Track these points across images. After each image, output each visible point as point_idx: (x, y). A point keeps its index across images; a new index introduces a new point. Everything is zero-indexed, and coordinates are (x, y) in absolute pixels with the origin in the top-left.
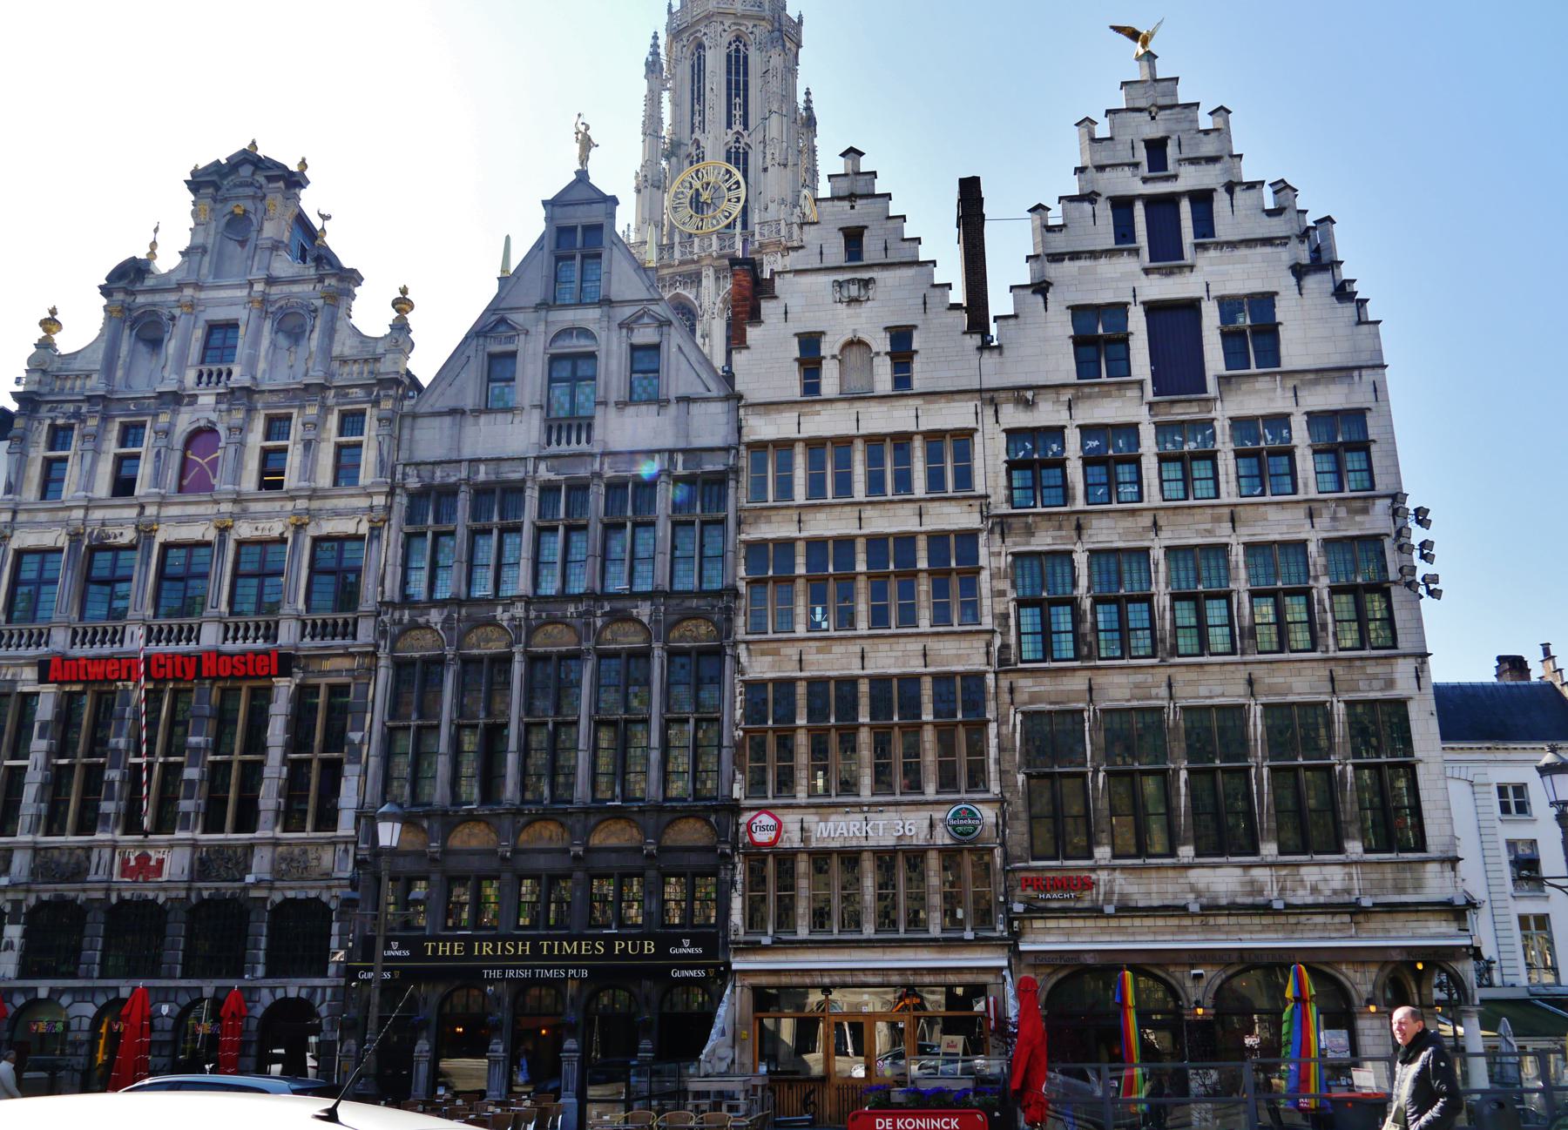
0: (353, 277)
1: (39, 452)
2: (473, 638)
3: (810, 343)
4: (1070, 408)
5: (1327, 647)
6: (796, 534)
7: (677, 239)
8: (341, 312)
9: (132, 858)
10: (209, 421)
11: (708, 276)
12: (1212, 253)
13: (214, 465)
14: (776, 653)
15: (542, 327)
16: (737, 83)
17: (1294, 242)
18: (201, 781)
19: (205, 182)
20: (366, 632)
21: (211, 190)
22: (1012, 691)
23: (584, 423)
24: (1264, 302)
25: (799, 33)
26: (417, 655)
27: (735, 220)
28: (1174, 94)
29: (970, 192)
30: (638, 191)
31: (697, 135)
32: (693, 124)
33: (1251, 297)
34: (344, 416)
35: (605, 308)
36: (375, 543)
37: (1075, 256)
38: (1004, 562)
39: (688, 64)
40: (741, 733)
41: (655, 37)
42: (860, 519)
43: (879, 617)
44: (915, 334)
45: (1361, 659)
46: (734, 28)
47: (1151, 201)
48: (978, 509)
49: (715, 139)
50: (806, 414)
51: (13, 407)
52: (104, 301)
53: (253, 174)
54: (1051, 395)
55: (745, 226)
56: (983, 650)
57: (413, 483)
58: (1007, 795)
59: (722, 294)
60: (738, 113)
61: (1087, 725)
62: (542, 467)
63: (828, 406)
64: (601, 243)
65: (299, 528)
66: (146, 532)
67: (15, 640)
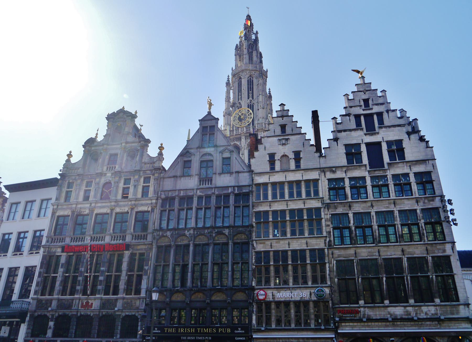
0: (148, 141)
1: (65, 190)
2: (179, 240)
3: (272, 156)
4: (346, 173)
5: (425, 240)
6: (269, 209)
7: (235, 129)
8: (145, 151)
9: (84, 302)
10: (109, 180)
12: (384, 129)
13: (110, 192)
14: (264, 243)
15: (198, 153)
16: (250, 87)
17: (407, 126)
18: (104, 280)
19: (111, 118)
20: (149, 238)
21: (112, 120)
22: (332, 254)
23: (210, 179)
24: (399, 142)
25: (267, 74)
26: (163, 244)
27: (250, 123)
28: (370, 87)
29: (315, 115)
30: (224, 116)
31: (240, 101)
32: (239, 98)
33: (396, 141)
34: (145, 178)
35: (215, 148)
36: (152, 213)
37: (345, 131)
38: (329, 216)
39: (237, 83)
40: (255, 267)
41: (228, 76)
42: (287, 205)
43: (293, 233)
44: (301, 153)
45: (435, 244)
47: (365, 115)
48: (320, 201)
49: (245, 102)
50: (271, 176)
51: (59, 177)
52: (84, 149)
53: (123, 115)
54: (340, 169)
55: (253, 124)
56: (324, 242)
57: (163, 196)
58: (333, 285)
60: (251, 95)
61: (355, 264)
62: (198, 191)
63: (277, 173)
64: (214, 130)
65: (132, 209)
66: (92, 211)
67: (56, 241)
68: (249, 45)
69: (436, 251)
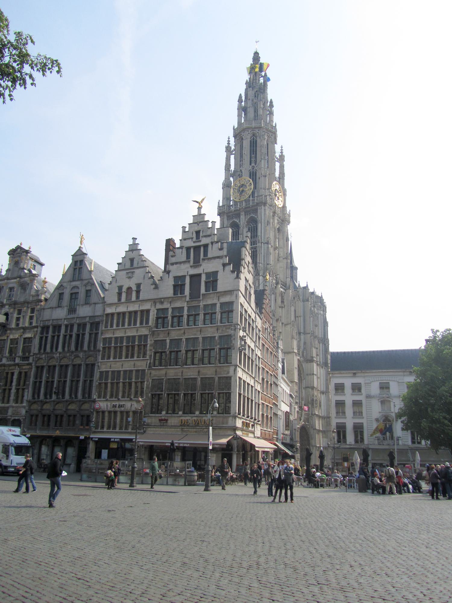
2: (50, 361)
3: (120, 288)
11: (242, 214)
12: (206, 261)
15: (69, 287)
16: (253, 149)
22: (150, 374)
24: (215, 273)
30: (223, 188)
33: (213, 272)
37: (176, 263)
38: (153, 342)
44: (141, 285)
46: (252, 132)
57: (41, 325)
59: (247, 219)
62: (65, 321)
68: (255, 94)
69: (222, 373)
